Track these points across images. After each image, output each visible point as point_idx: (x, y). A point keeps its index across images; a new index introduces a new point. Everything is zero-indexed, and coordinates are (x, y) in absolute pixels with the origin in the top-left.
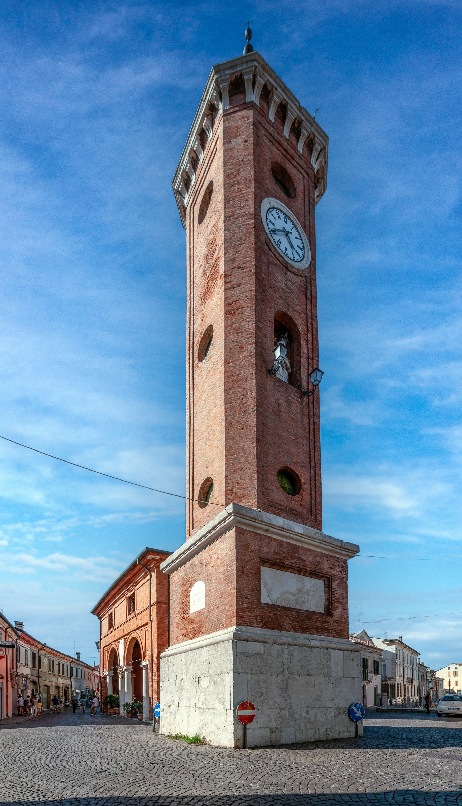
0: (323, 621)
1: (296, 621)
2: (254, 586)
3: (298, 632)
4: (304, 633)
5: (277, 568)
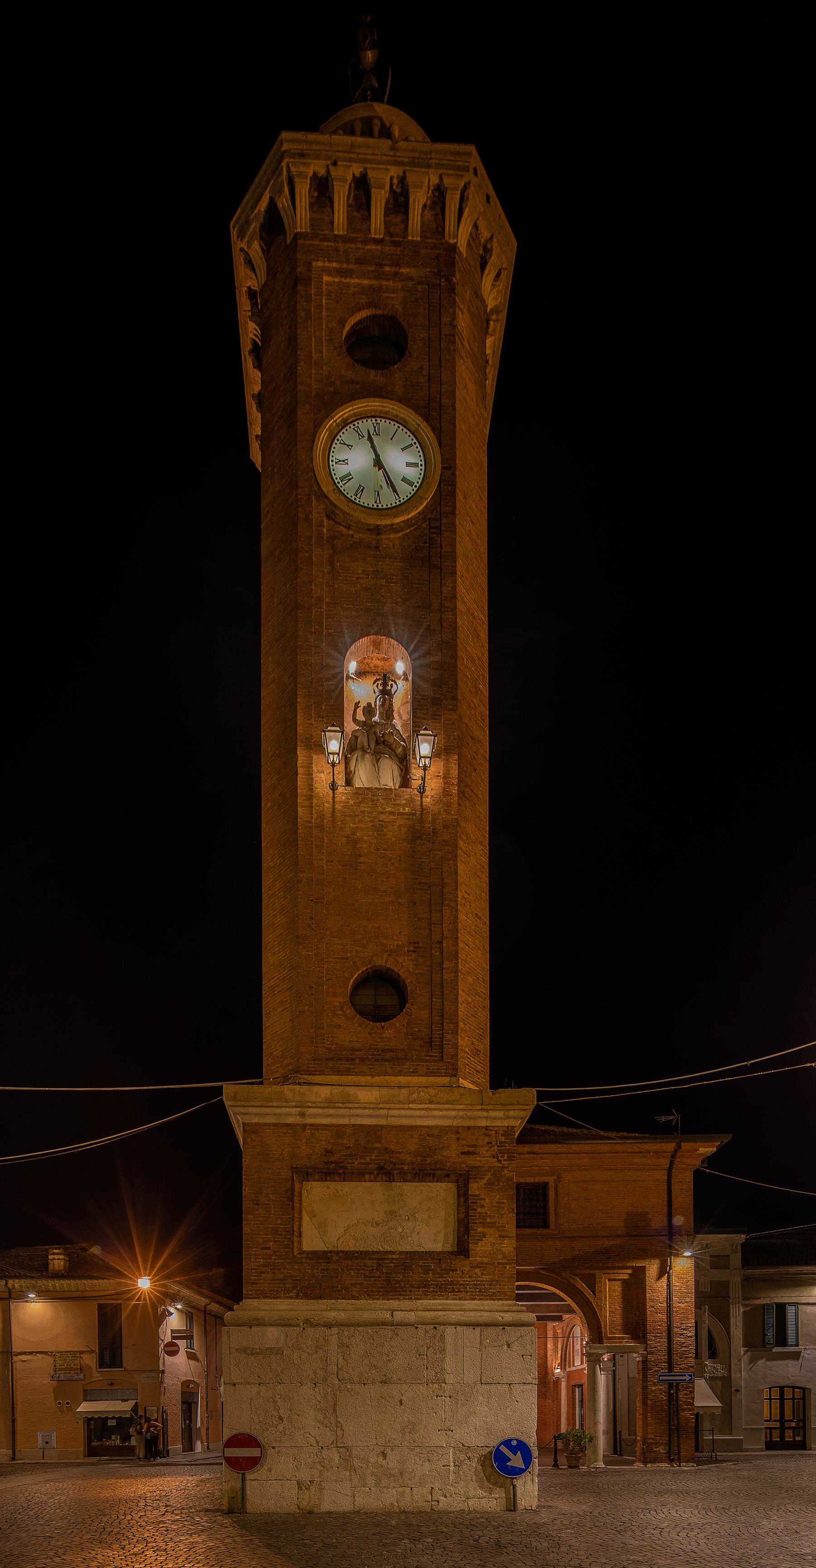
0: (441, 1270)
1: (374, 1277)
2: (279, 1224)
3: (378, 1299)
4: (392, 1299)
5: (337, 1178)
